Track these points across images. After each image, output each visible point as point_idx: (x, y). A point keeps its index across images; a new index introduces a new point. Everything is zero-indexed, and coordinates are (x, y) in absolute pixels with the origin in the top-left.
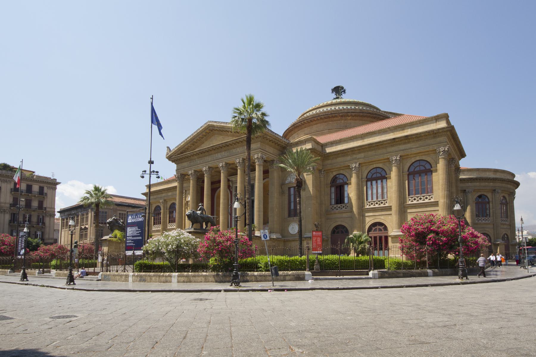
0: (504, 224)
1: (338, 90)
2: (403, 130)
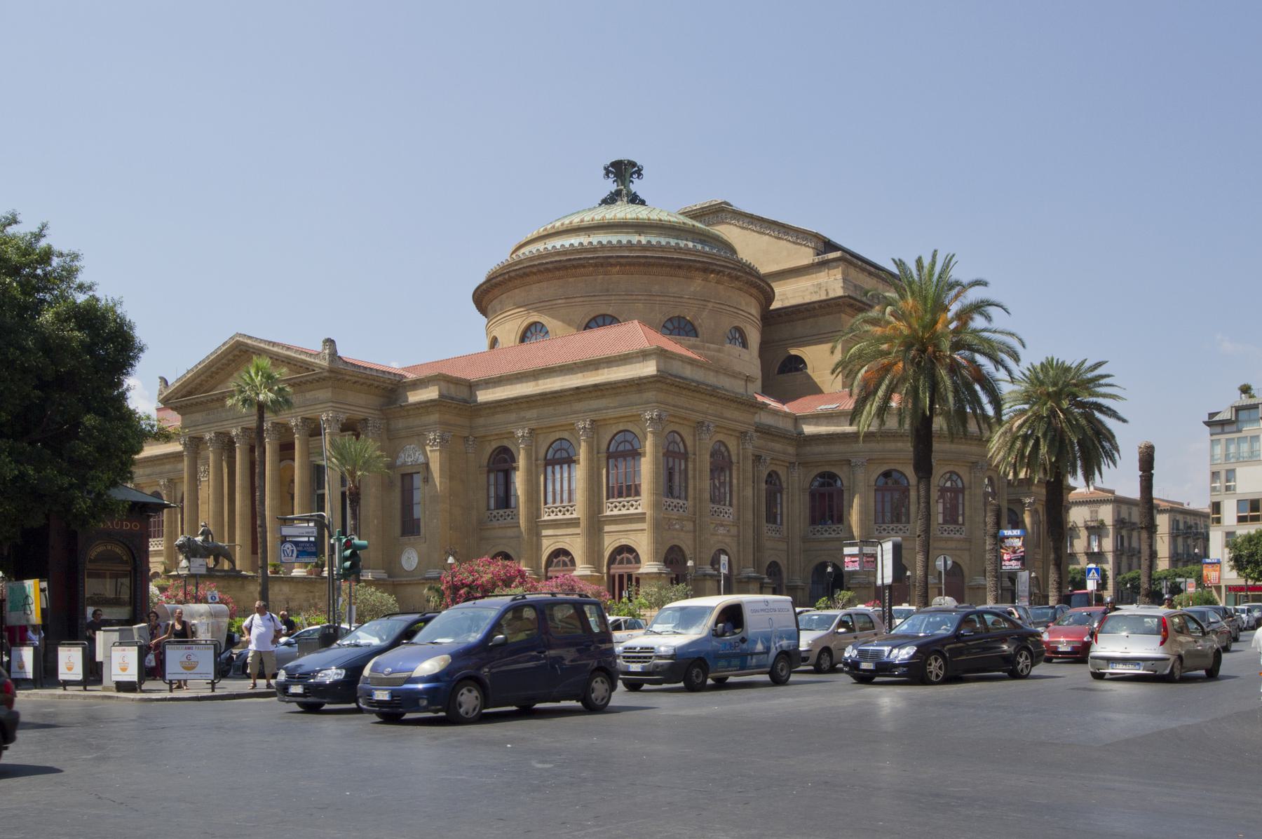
0: (947, 540)
1: (622, 170)
2: (597, 369)
